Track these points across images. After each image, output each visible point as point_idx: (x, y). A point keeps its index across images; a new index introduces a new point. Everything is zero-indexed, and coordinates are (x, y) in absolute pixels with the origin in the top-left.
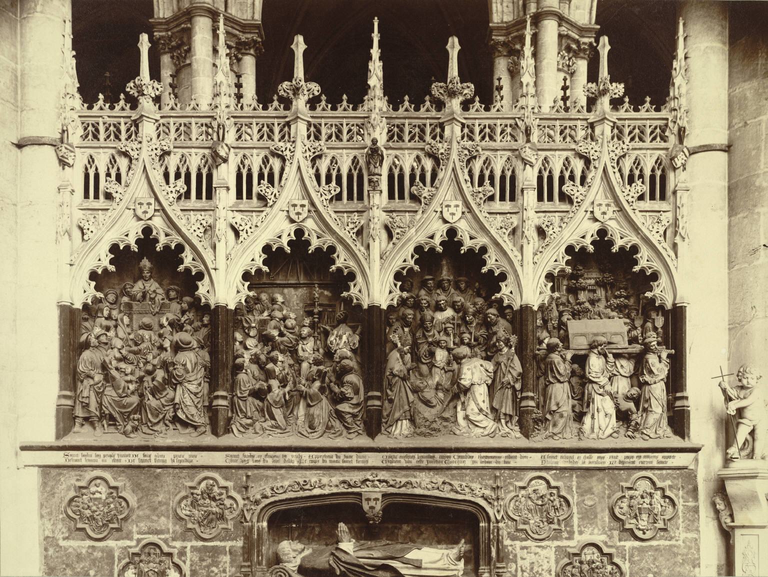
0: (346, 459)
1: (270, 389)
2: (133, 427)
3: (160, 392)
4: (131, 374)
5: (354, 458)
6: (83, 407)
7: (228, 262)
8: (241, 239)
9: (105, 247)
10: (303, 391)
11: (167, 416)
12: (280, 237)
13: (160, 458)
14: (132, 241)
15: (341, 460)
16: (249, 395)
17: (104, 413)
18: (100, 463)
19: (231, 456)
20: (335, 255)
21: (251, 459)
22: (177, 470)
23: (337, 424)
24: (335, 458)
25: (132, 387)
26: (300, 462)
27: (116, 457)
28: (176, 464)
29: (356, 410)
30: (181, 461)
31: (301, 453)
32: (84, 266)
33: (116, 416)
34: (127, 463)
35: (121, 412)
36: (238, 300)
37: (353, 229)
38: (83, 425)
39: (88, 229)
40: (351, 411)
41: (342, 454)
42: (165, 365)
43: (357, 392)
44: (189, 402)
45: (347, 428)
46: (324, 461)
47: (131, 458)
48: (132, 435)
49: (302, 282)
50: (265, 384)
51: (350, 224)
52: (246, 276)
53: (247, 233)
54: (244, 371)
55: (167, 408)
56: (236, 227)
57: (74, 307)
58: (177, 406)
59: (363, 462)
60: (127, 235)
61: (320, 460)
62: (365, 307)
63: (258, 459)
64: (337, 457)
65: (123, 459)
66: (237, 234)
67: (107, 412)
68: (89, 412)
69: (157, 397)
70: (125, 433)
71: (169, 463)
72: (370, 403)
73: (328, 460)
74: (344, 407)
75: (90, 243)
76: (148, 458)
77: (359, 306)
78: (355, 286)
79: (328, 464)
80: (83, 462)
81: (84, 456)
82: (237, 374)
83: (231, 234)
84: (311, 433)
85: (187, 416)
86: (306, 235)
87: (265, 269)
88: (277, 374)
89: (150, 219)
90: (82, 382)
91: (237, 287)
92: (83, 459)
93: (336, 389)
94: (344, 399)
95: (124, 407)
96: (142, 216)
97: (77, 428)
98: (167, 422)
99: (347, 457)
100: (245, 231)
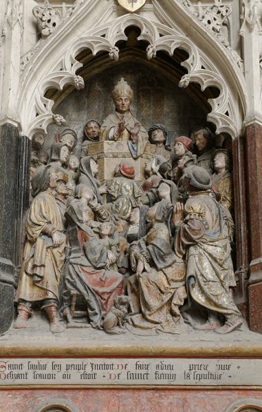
2: (118, 316)
3: (162, 258)
4: (110, 236)
6: (34, 284)
9: (69, 51)
11: (175, 301)
13: (165, 371)
14: (112, 40)
17: (68, 293)
18: (59, 380)
22: (190, 395)
25: (112, 256)
27: (89, 370)
28: (192, 381)
30: (201, 377)
32: (39, 77)
33: (89, 297)
34: (106, 381)
35: (97, 292)
38: (30, 316)
39: (49, 21)
42: (168, 216)
44: (209, 273)
47: (114, 372)
48: (117, 329)
55: (174, 285)
57: (22, 134)
58: (192, 281)
60: (104, 36)
65: (100, 373)
67: (74, 292)
68: (46, 291)
69: (159, 266)
70: (104, 328)
71: (180, 381)
75: (50, 40)
76: (143, 371)
80: (30, 380)
81: (32, 367)
85: (208, 299)
89: (137, 12)
90: (33, 242)
92: (30, 375)
95: (102, 283)
96: (129, 8)
97: (21, 320)
98: (176, 310)
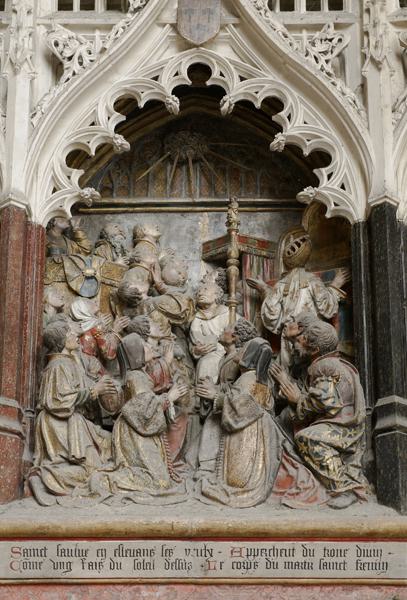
0: (328, 559)
1: (128, 393)
5: (351, 557)
7: (35, 121)
8: (67, 74)
10: (211, 401)
12: (156, 78)
15: (315, 561)
16: (77, 408)
19: (26, 552)
20: (283, 114)
21: (76, 561)
23: (302, 474)
24: (299, 557)
26: (206, 567)
29: (350, 441)
31: (210, 544)
36: (55, 204)
37: (325, 53)
40: (337, 440)
41: (318, 546)
43: (352, 402)
45: (328, 484)
46: (270, 565)
49: (198, 200)
50: (118, 384)
51: (318, 43)
52: (76, 158)
53: (81, 64)
54: (65, 352)
56: (56, 51)
59: (374, 566)
61: (261, 560)
62: (358, 214)
63: (99, 560)
64: (306, 552)
66: (56, 66)
72: (381, 424)
73: (281, 560)
74: (320, 432)
77: (340, 221)
78: (329, 176)
79: (282, 572)
82: (48, 360)
83: (44, 74)
84: (235, 494)
86: (215, 74)
87: (121, 141)
88: (148, 357)
91: (54, 178)
93: (294, 391)
94: (318, 413)
99: (332, 553)
100: (76, 58)
